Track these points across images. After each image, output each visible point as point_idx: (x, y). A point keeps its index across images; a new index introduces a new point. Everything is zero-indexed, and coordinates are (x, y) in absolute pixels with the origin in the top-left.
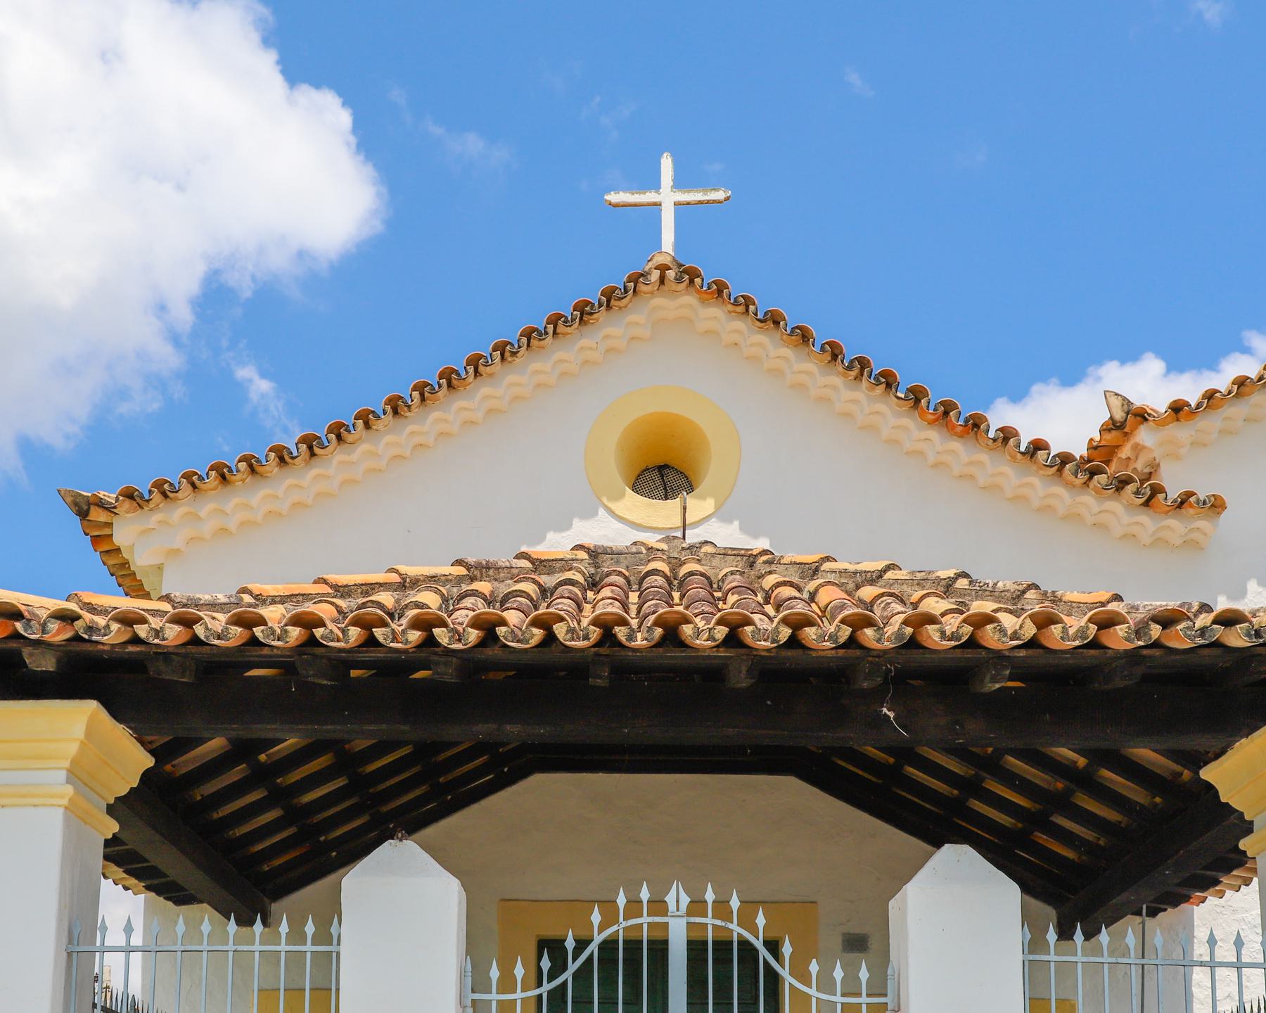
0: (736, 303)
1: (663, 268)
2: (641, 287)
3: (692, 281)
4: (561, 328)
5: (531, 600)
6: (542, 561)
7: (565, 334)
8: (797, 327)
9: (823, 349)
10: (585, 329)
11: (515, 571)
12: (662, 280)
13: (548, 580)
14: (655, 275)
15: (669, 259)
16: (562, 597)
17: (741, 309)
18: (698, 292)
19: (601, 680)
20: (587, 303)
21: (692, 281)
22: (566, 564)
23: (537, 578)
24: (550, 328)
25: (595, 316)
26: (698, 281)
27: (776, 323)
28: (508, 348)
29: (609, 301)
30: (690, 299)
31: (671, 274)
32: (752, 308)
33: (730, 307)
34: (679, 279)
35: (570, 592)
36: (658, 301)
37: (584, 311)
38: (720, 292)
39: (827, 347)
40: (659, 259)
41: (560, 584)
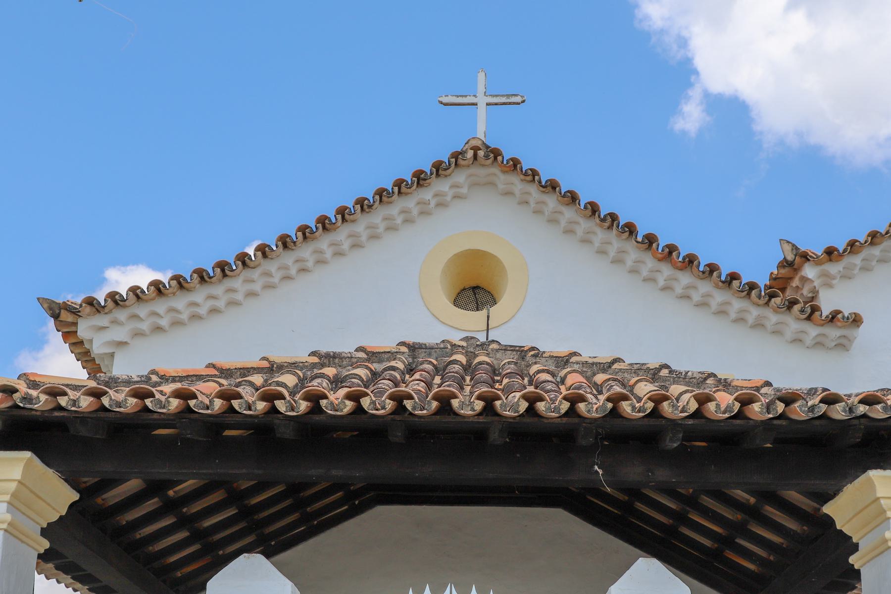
0: (526, 174)
1: (476, 149)
2: (461, 162)
3: (495, 158)
4: (403, 189)
5: (362, 380)
6: (374, 353)
7: (407, 194)
8: (568, 192)
9: (585, 207)
10: (420, 190)
11: (354, 360)
12: (475, 156)
13: (376, 367)
14: (470, 154)
15: (480, 142)
16: (384, 379)
17: (530, 178)
18: (500, 166)
19: (397, 436)
20: (422, 172)
21: (495, 158)
22: (393, 355)
23: (370, 365)
24: (396, 189)
25: (428, 181)
26: (499, 158)
27: (554, 188)
28: (366, 202)
29: (437, 171)
30: (495, 170)
31: (481, 153)
32: (537, 178)
33: (522, 177)
34: (486, 157)
35: (391, 375)
36: (473, 170)
37: (420, 178)
38: (515, 166)
39: (589, 207)
40: (474, 143)
41: (385, 370)
